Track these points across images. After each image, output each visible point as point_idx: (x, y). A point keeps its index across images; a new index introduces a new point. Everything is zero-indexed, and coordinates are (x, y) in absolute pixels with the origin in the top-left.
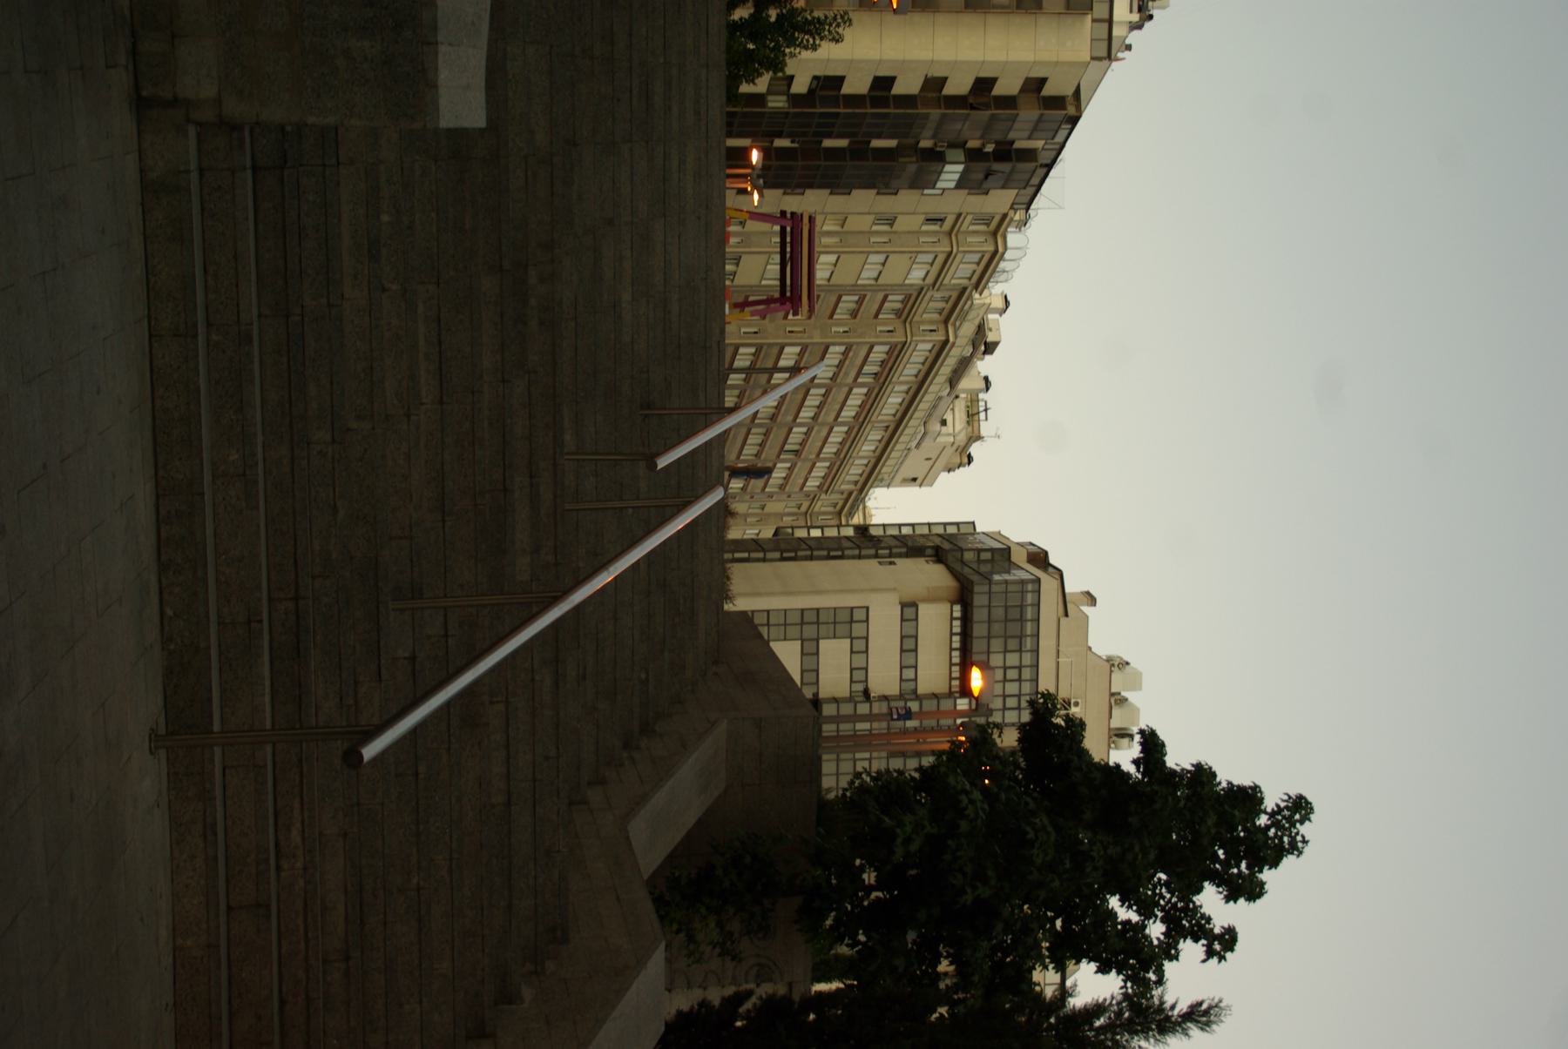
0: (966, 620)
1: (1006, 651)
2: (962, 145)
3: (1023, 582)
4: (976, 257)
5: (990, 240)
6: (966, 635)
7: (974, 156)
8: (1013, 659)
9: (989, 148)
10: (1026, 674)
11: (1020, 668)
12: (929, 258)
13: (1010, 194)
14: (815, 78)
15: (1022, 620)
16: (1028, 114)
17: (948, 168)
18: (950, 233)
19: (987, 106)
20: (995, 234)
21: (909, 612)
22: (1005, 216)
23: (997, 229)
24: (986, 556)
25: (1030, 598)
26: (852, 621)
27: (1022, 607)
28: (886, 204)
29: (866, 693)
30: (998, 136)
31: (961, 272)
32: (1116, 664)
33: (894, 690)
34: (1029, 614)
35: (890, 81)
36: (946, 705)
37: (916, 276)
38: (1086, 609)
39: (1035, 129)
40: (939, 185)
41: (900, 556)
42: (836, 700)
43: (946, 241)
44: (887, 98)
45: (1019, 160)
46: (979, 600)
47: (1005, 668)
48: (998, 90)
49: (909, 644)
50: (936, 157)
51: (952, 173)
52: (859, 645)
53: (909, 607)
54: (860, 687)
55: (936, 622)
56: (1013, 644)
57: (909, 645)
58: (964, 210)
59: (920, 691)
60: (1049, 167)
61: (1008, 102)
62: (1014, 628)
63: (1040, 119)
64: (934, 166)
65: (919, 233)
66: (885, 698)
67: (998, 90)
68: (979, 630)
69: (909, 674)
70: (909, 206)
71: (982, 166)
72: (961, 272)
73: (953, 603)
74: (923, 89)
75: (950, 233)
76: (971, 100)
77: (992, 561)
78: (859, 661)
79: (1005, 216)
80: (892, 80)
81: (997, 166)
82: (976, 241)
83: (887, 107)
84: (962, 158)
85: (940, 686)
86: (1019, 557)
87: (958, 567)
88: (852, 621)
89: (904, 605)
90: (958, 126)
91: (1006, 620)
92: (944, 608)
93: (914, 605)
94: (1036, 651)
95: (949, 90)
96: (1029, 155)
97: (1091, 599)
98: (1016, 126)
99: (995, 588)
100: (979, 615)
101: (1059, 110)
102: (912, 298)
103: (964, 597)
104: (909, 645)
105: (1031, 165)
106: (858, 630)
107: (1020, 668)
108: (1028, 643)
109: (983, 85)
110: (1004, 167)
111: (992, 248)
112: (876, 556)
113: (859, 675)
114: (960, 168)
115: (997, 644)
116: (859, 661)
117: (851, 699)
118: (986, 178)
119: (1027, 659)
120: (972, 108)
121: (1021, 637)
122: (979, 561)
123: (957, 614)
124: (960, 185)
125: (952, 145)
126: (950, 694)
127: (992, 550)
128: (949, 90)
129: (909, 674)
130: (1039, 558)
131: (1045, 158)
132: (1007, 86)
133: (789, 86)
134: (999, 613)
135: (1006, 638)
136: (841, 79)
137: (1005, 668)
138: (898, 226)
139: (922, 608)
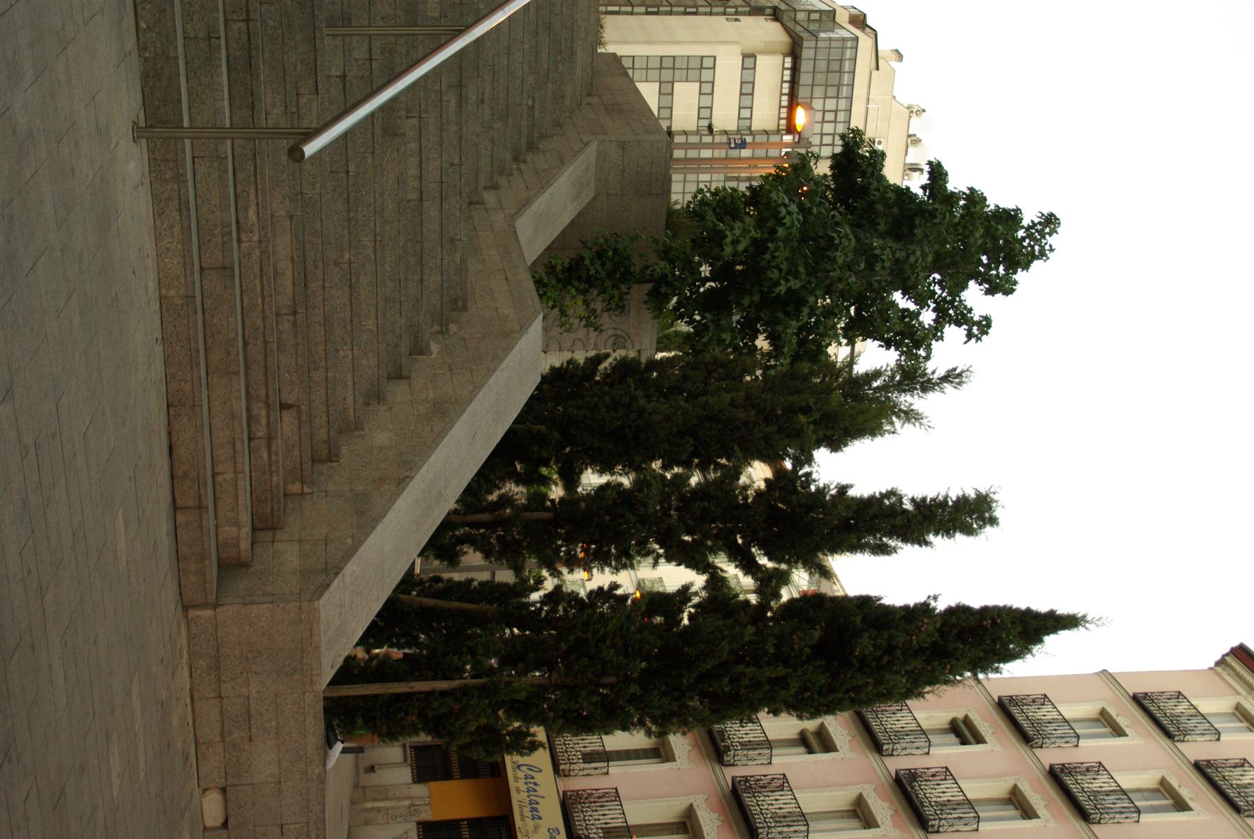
0: (795, 70)
1: (826, 97)
3: (844, 40)
6: (794, 82)
8: (831, 104)
11: (836, 112)
15: (841, 72)
21: (749, 62)
24: (815, 16)
25: (848, 54)
26: (702, 68)
27: (841, 61)
29: (710, 128)
32: (915, 111)
33: (732, 126)
34: (847, 66)
38: (894, 64)
41: (744, 14)
42: (685, 133)
46: (807, 54)
49: (747, 89)
52: (707, 88)
53: (749, 57)
54: (706, 123)
55: (771, 71)
56: (832, 91)
57: (747, 90)
62: (833, 78)
66: (726, 132)
68: (805, 79)
69: (746, 113)
73: (785, 55)
77: (820, 20)
78: (706, 101)
85: (771, 126)
86: (842, 18)
87: (791, 25)
88: (702, 68)
89: (745, 56)
91: (828, 71)
92: (777, 59)
93: (753, 56)
97: (899, 56)
99: (820, 44)
100: (806, 66)
103: (794, 52)
104: (747, 90)
106: (706, 75)
107: (836, 112)
108: (845, 91)
112: (724, 14)
113: (705, 113)
115: (819, 91)
116: (706, 101)
117: (697, 132)
119: (843, 104)
121: (839, 86)
122: (809, 20)
123: (788, 65)
126: (778, 131)
127: (820, 12)
129: (746, 113)
130: (859, 21)
134: (822, 65)
135: (827, 86)
137: (824, 112)
139: (759, 58)
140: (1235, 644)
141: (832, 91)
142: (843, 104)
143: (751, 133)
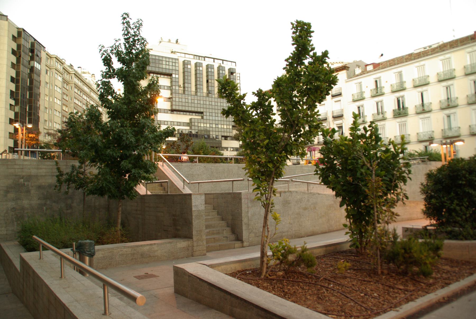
2: (29, 62)
4: (56, 63)
5: (52, 59)
7: (32, 58)
8: (164, 63)
9: (30, 54)
10: (167, 60)
11: (166, 61)
12: (56, 75)
13: (42, 51)
14: (11, 98)
16: (22, 42)
17: (35, 66)
18: (50, 69)
19: (20, 53)
20: (51, 57)
22: (47, 54)
23: (49, 56)
28: (43, 84)
30: (28, 51)
31: (59, 67)
35: (12, 78)
36: (174, 80)
37: (60, 79)
39: (26, 41)
40: (39, 69)
42: (172, 106)
43: (52, 70)
44: (17, 79)
45: (34, 47)
47: (166, 65)
48: (15, 49)
50: (32, 69)
51: (37, 65)
56: (161, 62)
58: (45, 64)
59: (170, 85)
60: (35, 40)
61: (19, 46)
63: (24, 39)
64: (35, 69)
65: (50, 76)
66: (171, 94)
67: (15, 49)
69: (166, 88)
70: (44, 78)
71: (35, 57)
72: (59, 67)
74: (14, 69)
75: (50, 69)
76: (18, 56)
79: (47, 54)
80: (12, 77)
81: (35, 53)
82: (53, 63)
83: (19, 79)
84: (33, 62)
90: (25, 61)
94: (162, 57)
95: (15, 62)
96: (33, 45)
98: (25, 45)
101: (20, 34)
102: (65, 81)
105: (36, 44)
107: (166, 61)
108: (161, 58)
109: (14, 52)
110: (36, 51)
111: (55, 59)
114: (35, 63)
115: (161, 66)
118: (38, 56)
119: (164, 59)
120: (20, 56)
121: (159, 60)
124: (39, 63)
125: (29, 64)
126: (171, 79)
128: (15, 62)
129: (166, 88)
131: (33, 41)
132: (15, 47)
133: (13, 105)
135: (159, 64)
136: (11, 91)
137: (166, 65)
138: (48, 82)
140: (306, 21)
141: (161, 62)
142: (164, 59)
143: (172, 86)
